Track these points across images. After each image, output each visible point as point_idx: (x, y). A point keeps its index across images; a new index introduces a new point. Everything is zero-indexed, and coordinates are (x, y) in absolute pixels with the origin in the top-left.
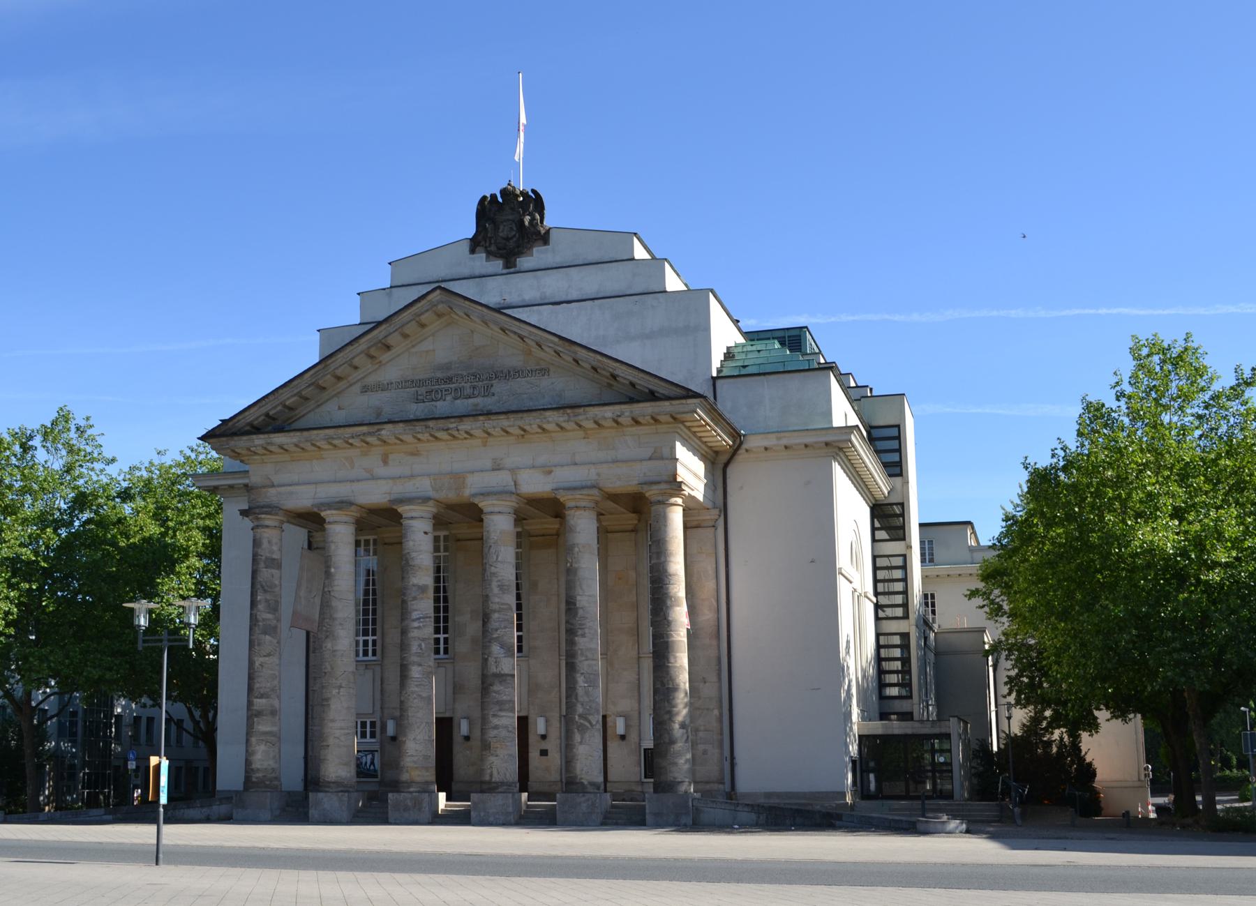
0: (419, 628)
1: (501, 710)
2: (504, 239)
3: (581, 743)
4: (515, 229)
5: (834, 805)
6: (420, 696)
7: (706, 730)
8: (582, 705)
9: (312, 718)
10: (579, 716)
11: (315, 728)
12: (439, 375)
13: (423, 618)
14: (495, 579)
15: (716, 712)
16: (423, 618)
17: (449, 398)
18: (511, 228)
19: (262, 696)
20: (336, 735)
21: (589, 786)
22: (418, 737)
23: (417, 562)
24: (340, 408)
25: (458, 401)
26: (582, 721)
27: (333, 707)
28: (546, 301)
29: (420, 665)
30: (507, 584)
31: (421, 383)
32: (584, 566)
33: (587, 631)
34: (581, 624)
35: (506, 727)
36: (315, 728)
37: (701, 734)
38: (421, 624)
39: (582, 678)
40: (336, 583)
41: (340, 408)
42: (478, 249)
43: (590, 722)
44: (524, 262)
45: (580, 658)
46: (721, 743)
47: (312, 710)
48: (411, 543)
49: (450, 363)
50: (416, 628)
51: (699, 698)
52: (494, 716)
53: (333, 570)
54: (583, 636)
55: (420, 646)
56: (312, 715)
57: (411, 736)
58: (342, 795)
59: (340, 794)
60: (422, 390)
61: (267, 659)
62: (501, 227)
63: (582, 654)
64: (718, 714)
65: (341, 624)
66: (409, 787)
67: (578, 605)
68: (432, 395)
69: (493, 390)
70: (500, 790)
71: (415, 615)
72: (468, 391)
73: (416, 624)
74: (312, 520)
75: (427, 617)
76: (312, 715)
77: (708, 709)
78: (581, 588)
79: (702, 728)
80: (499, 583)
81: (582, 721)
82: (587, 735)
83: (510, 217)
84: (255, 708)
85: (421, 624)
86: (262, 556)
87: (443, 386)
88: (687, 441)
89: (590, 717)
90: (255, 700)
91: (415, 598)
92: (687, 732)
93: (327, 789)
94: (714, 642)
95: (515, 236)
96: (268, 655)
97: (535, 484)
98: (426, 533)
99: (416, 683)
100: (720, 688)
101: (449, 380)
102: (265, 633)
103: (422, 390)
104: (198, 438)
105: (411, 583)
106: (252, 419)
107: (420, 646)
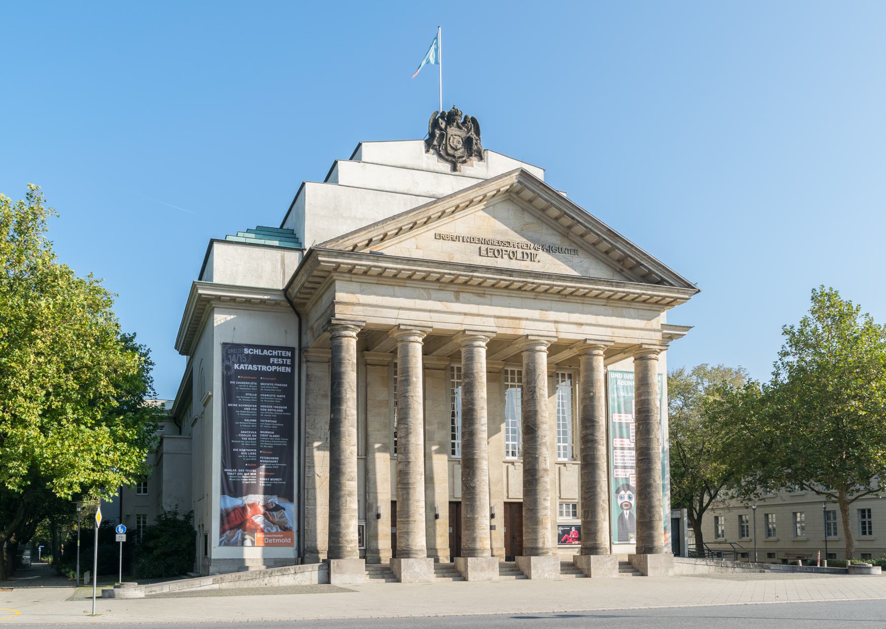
9: (308, 499)
11: (310, 507)
24: (417, 248)
36: (310, 507)
41: (417, 248)
47: (308, 493)
56: (307, 496)
58: (430, 561)
60: (484, 247)
76: (307, 496)
84: (347, 489)
86: (349, 360)
87: (501, 247)
90: (347, 482)
93: (414, 556)
105: (480, 396)
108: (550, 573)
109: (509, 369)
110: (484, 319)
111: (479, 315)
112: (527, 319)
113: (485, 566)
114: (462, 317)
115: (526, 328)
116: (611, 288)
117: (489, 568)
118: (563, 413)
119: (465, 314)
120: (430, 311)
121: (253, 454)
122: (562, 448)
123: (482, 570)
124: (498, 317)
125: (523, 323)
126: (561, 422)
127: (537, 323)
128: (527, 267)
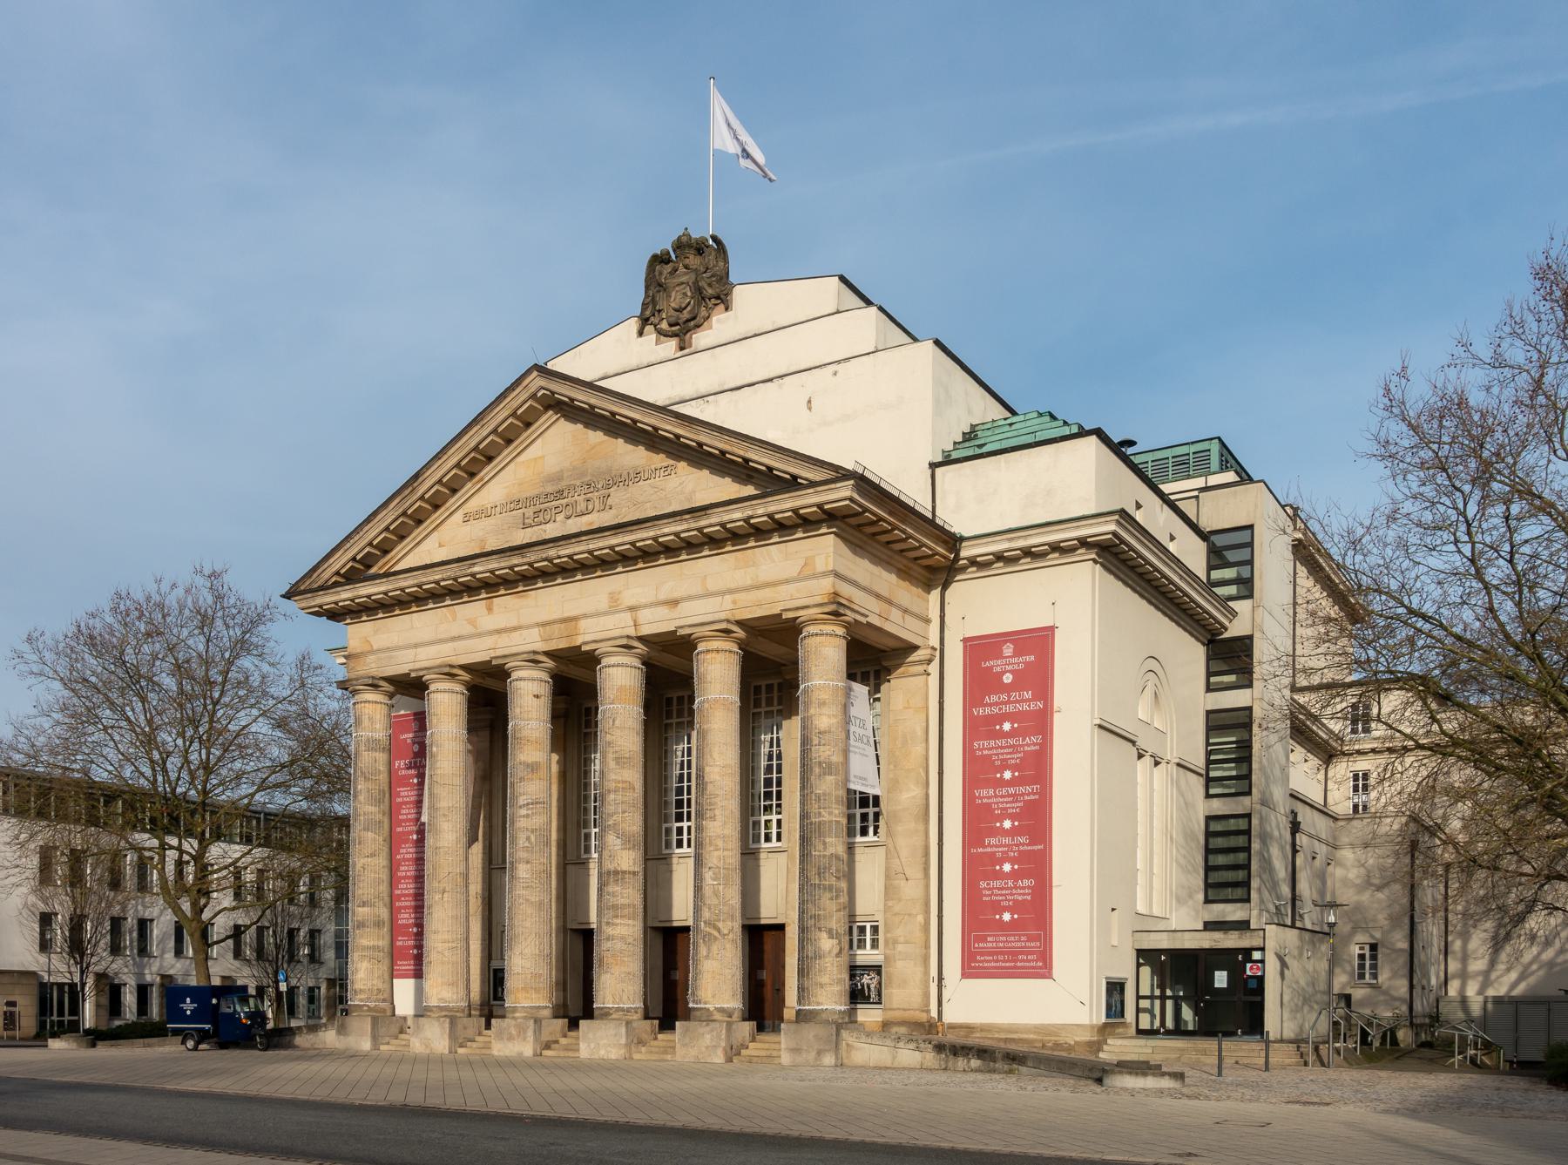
0: (527, 816)
1: (617, 917)
2: (676, 310)
3: (707, 957)
4: (689, 294)
5: (1072, 1043)
6: (527, 900)
7: (906, 942)
8: (710, 909)
10: (705, 922)
12: (550, 489)
13: (532, 804)
14: (611, 750)
15: (920, 918)
16: (532, 804)
17: (560, 517)
18: (685, 294)
19: (364, 904)
20: (440, 950)
21: (715, 1012)
22: (527, 951)
23: (525, 733)
24: (440, 546)
25: (570, 521)
26: (708, 929)
27: (435, 915)
28: (726, 388)
29: (528, 862)
30: (627, 755)
31: (530, 501)
32: (716, 726)
33: (717, 812)
34: (711, 804)
35: (623, 938)
37: (900, 947)
38: (530, 812)
39: (711, 873)
40: (438, 765)
41: (440, 546)
42: (649, 328)
43: (719, 931)
44: (700, 338)
45: (709, 848)
46: (926, 959)
48: (518, 710)
49: (562, 471)
50: (524, 816)
51: (900, 900)
52: (608, 923)
53: (434, 749)
54: (713, 818)
55: (528, 838)
57: (517, 950)
59: (442, 1019)
61: (370, 860)
62: (673, 294)
63: (711, 844)
64: (923, 921)
65: (444, 815)
66: (514, 1012)
67: (706, 779)
68: (540, 517)
69: (610, 501)
70: (613, 1016)
71: (522, 800)
72: (581, 507)
73: (523, 812)
74: (411, 687)
75: (537, 803)
77: (909, 915)
78: (711, 756)
79: (902, 939)
80: (617, 755)
81: (708, 929)
82: (715, 948)
83: (684, 279)
85: (530, 812)
88: (860, 547)
89: (720, 925)
91: (522, 779)
92: (840, 943)
94: (921, 827)
95: (689, 303)
96: (373, 855)
97: (657, 622)
98: (537, 696)
99: (525, 885)
100: (927, 886)
101: (560, 494)
102: (367, 829)
103: (530, 512)
104: (283, 596)
106: (337, 567)
107: (528, 838)
108: (609, 1049)
109: (763, 683)
110: (525, 632)
111: (515, 629)
112: (585, 616)
113: (514, 1032)
114: (496, 637)
115: (587, 635)
116: (685, 526)
117: (519, 1036)
118: (689, 767)
119: (499, 632)
120: (453, 639)
121: (408, 874)
122: (774, 824)
123: (510, 1038)
124: (544, 624)
125: (583, 624)
126: (775, 775)
127: (602, 619)
128: (591, 524)
